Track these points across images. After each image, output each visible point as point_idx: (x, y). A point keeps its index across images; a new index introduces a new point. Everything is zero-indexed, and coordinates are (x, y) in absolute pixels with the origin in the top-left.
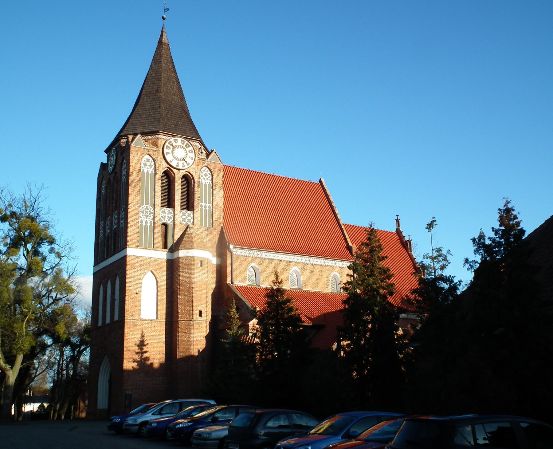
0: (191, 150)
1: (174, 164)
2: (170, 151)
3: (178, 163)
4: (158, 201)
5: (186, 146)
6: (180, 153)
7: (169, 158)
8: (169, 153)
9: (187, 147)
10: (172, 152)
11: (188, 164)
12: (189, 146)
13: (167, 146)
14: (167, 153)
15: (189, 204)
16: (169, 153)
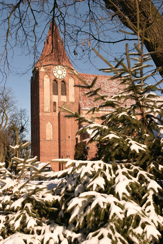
0: (65, 70)
1: (57, 77)
2: (56, 72)
3: (59, 76)
4: (52, 93)
5: (62, 69)
6: (60, 72)
7: (55, 75)
8: (55, 73)
9: (63, 69)
10: (57, 72)
11: (63, 77)
12: (64, 69)
13: (54, 70)
14: (54, 73)
15: (65, 92)
16: (55, 73)
